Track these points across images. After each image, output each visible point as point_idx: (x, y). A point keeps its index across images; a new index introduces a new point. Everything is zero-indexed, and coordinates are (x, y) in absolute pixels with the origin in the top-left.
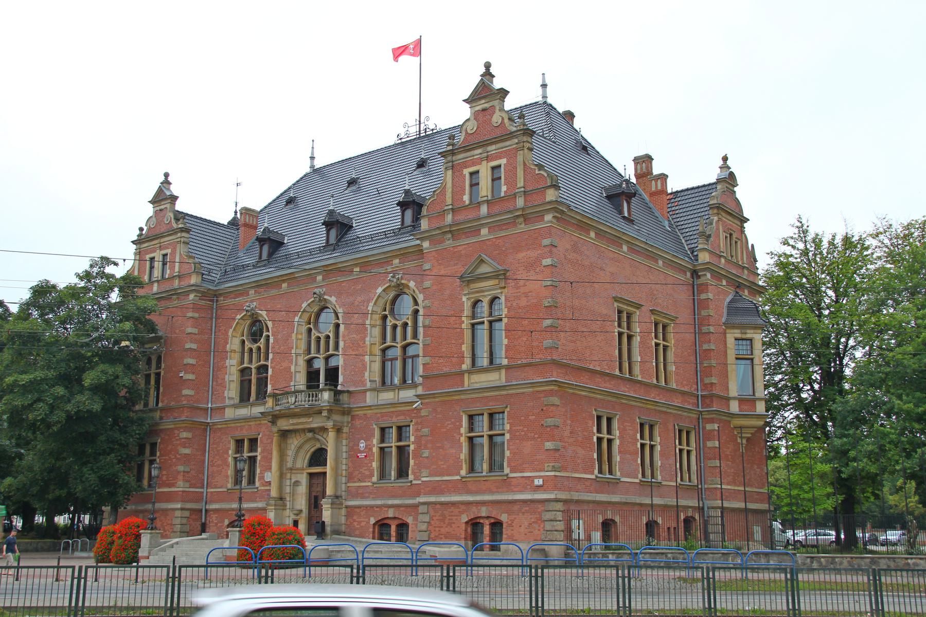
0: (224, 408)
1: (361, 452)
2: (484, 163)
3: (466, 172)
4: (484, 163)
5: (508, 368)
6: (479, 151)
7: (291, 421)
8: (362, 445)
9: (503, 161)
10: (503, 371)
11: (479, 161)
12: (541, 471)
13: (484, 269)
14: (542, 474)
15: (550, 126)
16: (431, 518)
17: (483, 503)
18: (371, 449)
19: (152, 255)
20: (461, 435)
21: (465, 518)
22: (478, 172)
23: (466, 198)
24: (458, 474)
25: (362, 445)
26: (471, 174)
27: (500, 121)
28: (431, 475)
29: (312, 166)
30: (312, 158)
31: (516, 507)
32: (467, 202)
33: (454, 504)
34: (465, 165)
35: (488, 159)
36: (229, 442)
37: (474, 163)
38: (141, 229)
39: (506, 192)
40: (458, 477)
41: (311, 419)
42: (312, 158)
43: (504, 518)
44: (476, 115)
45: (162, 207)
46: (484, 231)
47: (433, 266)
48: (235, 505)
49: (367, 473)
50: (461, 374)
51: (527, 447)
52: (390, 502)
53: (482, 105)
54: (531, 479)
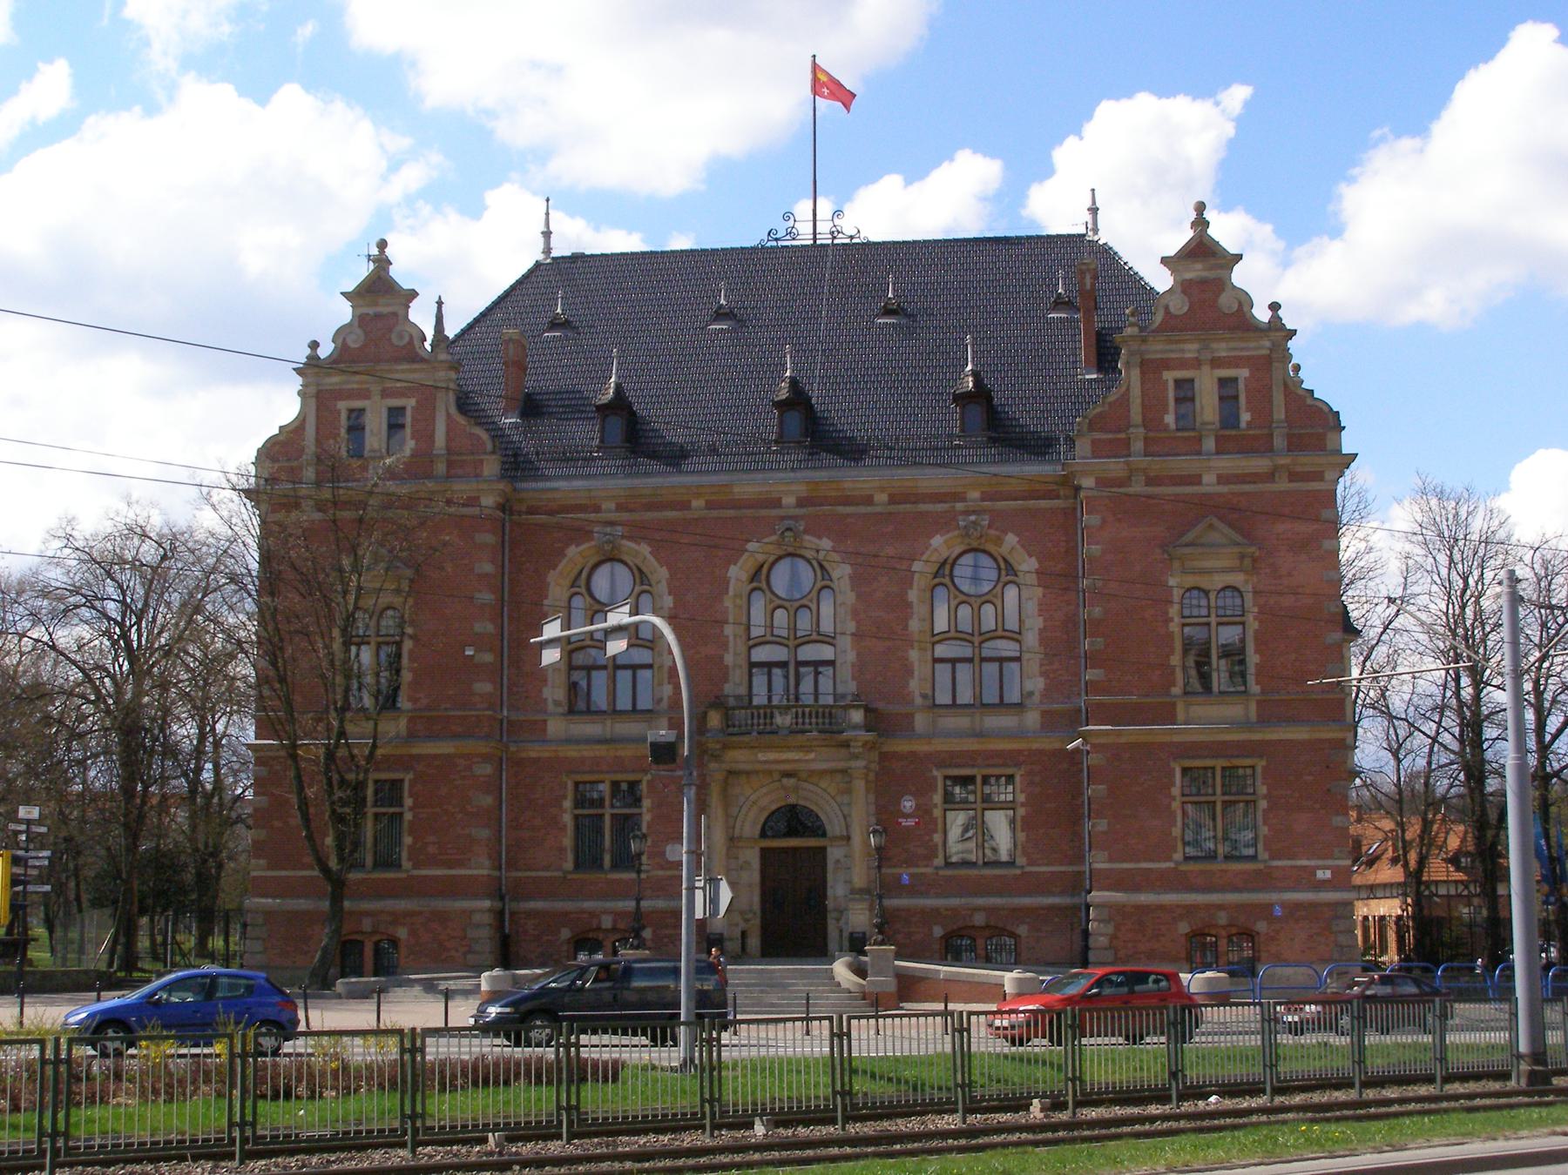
1: (906, 816)
2: (1206, 368)
3: (1169, 376)
4: (1206, 368)
6: (1195, 346)
7: (761, 756)
8: (908, 804)
9: (1243, 373)
10: (1253, 707)
11: (1197, 363)
12: (1326, 857)
14: (1330, 862)
15: (243, 92)
16: (1117, 928)
17: (1221, 907)
18: (928, 812)
20: (1174, 798)
21: (1184, 928)
22: (1192, 381)
23: (1170, 419)
24: (1169, 859)
25: (908, 804)
26: (1179, 383)
27: (1235, 307)
28: (1111, 860)
29: (547, 250)
30: (547, 234)
32: (1173, 426)
33: (1161, 907)
34: (1166, 364)
35: (1216, 363)
37: (1183, 364)
38: (314, 345)
39: (1249, 423)
40: (1170, 865)
41: (812, 756)
42: (547, 234)
44: (1184, 287)
47: (1104, 521)
48: (630, 905)
52: (980, 901)
53: (1196, 271)
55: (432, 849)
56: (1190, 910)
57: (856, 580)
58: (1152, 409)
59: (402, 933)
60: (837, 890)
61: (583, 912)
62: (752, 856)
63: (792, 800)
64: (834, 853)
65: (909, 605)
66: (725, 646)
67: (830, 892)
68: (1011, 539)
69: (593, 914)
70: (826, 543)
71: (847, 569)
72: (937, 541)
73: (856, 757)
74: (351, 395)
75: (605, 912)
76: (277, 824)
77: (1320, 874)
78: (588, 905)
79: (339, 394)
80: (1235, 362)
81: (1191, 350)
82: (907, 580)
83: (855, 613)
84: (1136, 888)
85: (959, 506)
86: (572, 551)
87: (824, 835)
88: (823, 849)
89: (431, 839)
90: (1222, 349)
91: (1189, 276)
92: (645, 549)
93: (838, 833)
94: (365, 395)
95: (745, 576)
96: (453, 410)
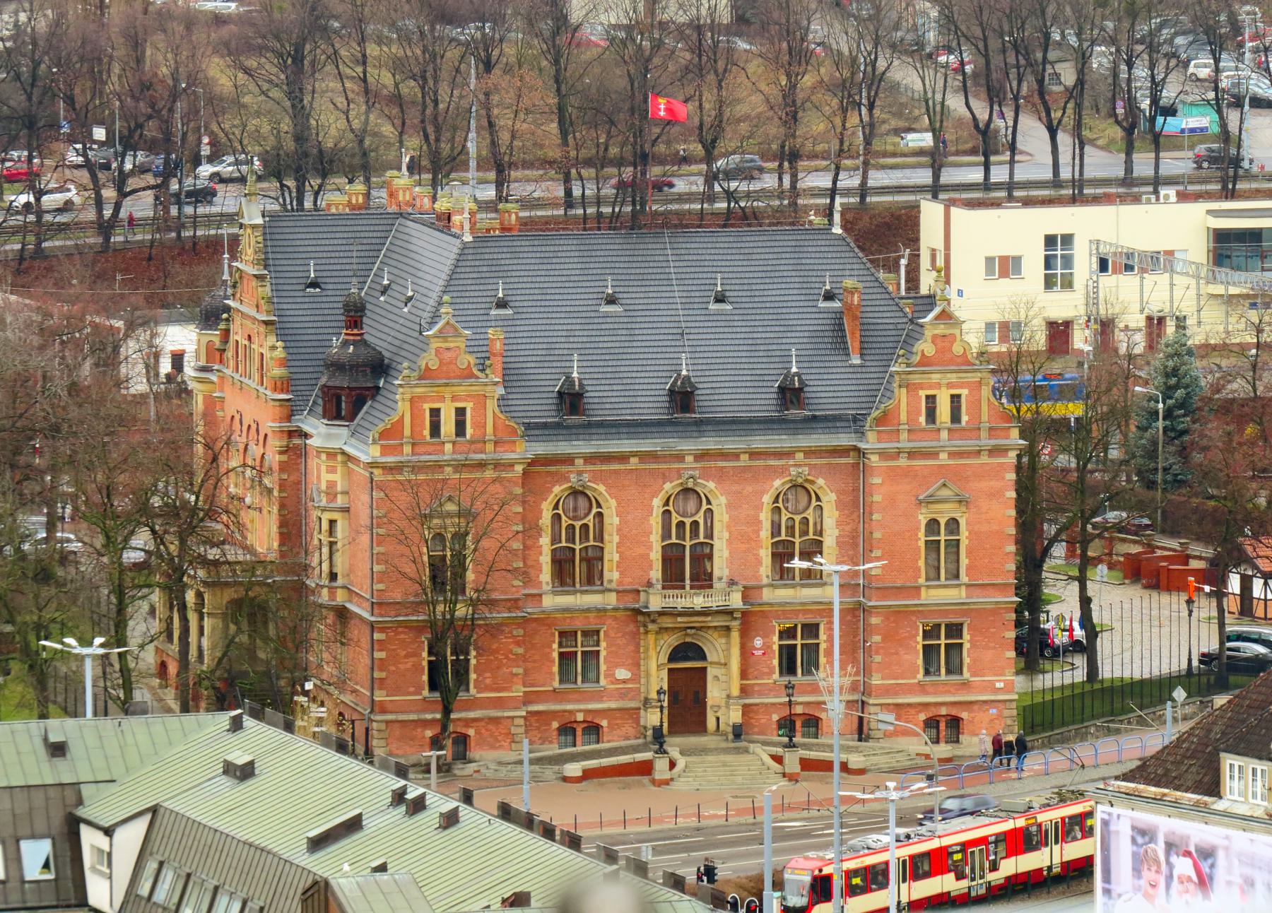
0: (540, 595)
2: (944, 389)
4: (944, 389)
5: (968, 586)
6: (938, 376)
7: (679, 619)
11: (938, 386)
13: (945, 493)
18: (770, 647)
19: (436, 406)
24: (915, 677)
25: (758, 642)
31: (976, 707)
33: (909, 705)
34: (921, 386)
35: (950, 385)
36: (553, 635)
37: (930, 387)
43: (964, 715)
45: (452, 345)
46: (943, 456)
49: (766, 670)
50: (918, 588)
51: (988, 655)
54: (993, 682)
55: (488, 681)
56: (926, 705)
57: (729, 506)
58: (913, 413)
59: (471, 732)
60: (714, 693)
61: (565, 711)
62: (665, 674)
63: (688, 640)
64: (711, 672)
65: (760, 522)
66: (650, 548)
67: (709, 694)
68: (821, 482)
69: (570, 712)
70: (711, 485)
71: (723, 500)
72: (777, 483)
73: (736, 619)
74: (433, 400)
75: (580, 711)
76: (393, 668)
77: (999, 685)
78: (569, 707)
79: (423, 398)
80: (960, 386)
81: (935, 378)
82: (759, 507)
83: (728, 527)
84: (896, 694)
85: (791, 462)
86: (557, 489)
87: (704, 658)
88: (705, 669)
89: (488, 675)
90: (953, 378)
91: (937, 332)
92: (601, 488)
93: (716, 660)
94: (442, 399)
95: (661, 503)
96: (497, 410)
